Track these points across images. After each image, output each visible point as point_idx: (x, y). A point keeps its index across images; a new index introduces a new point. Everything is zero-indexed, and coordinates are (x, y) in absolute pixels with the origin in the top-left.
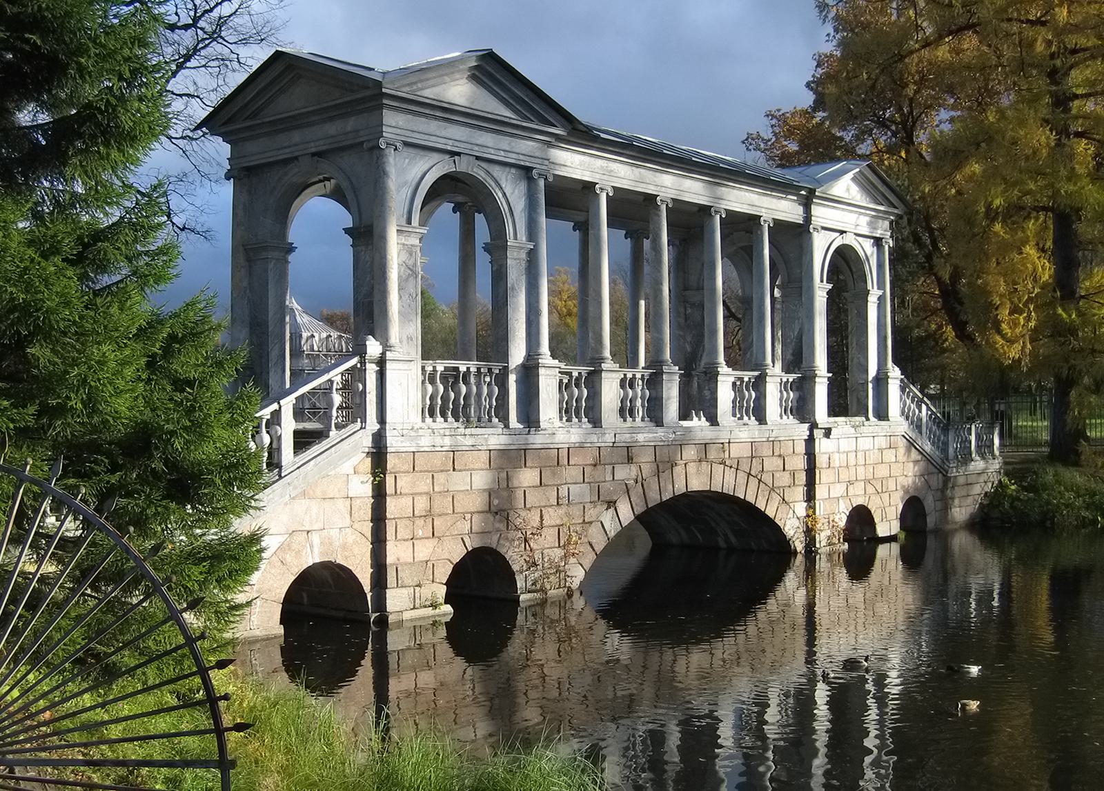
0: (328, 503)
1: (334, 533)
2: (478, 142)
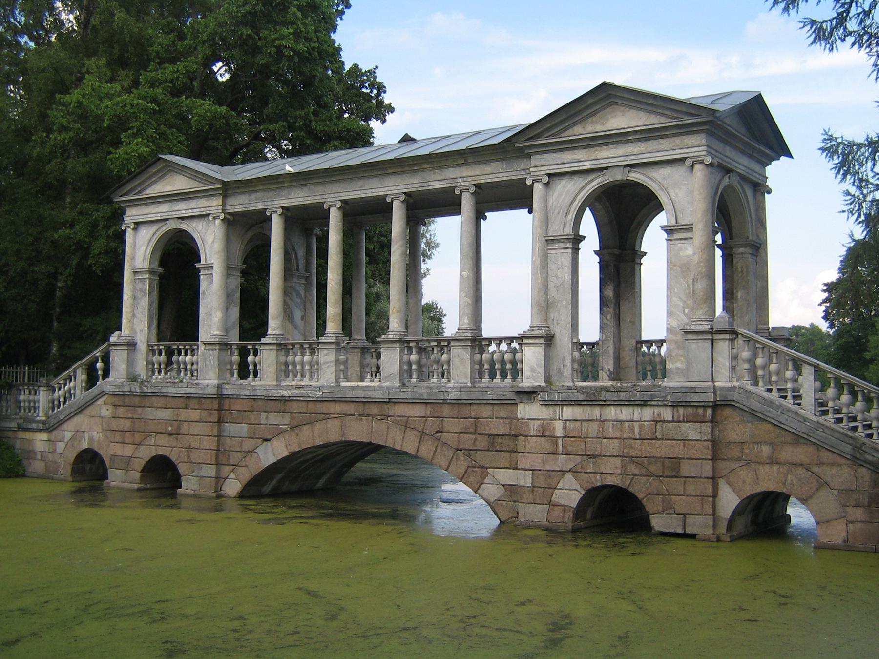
0: (92, 419)
1: (95, 434)
2: (176, 209)
